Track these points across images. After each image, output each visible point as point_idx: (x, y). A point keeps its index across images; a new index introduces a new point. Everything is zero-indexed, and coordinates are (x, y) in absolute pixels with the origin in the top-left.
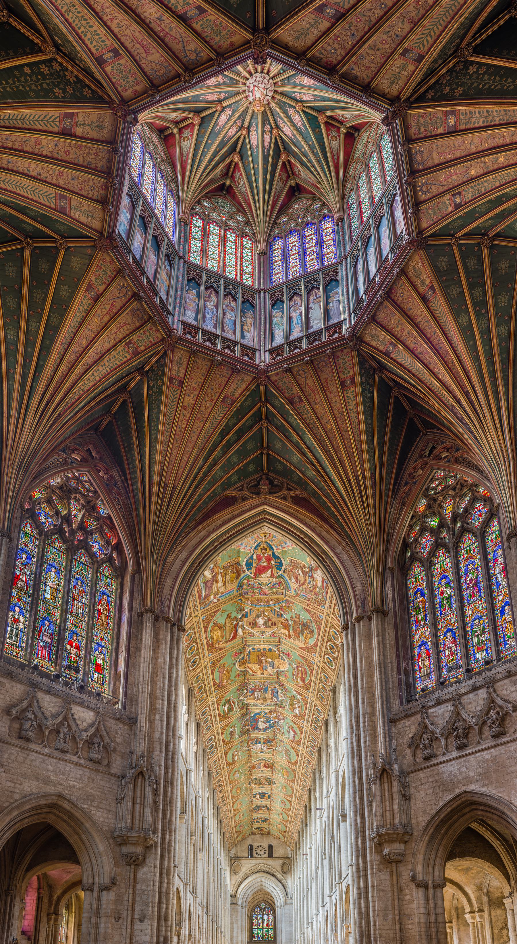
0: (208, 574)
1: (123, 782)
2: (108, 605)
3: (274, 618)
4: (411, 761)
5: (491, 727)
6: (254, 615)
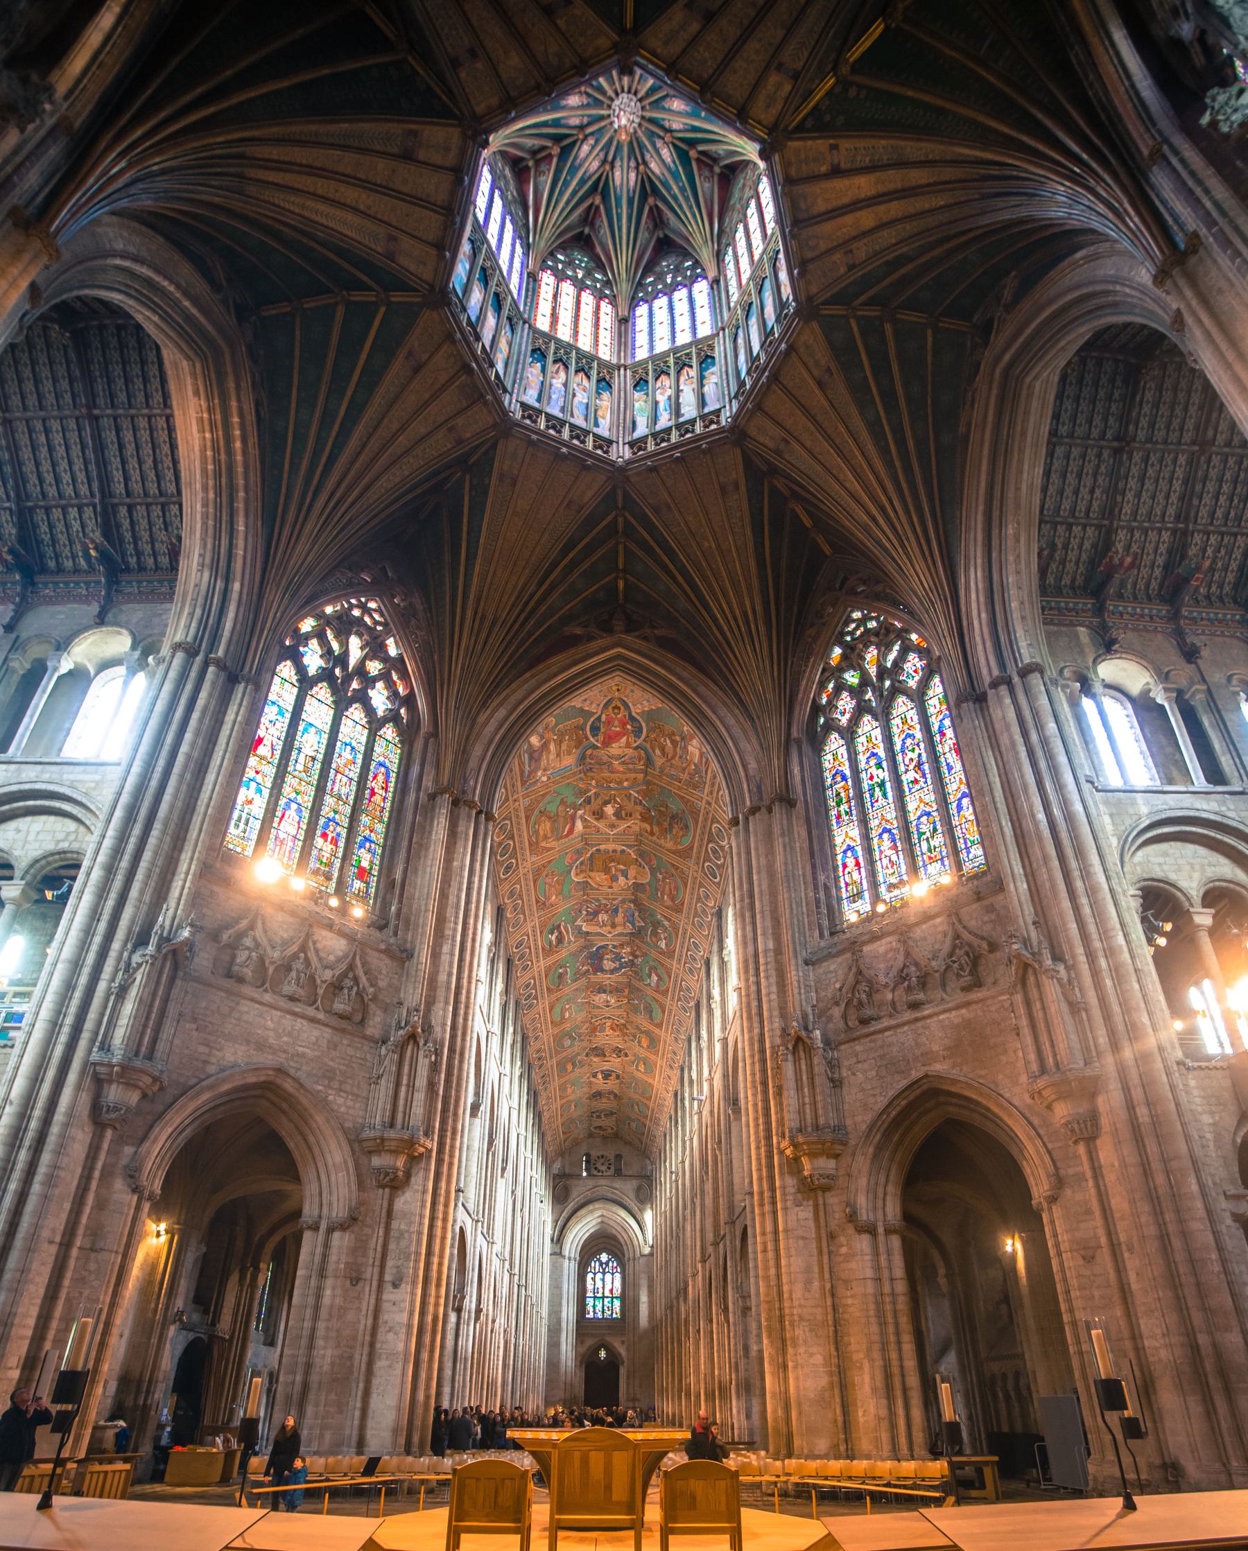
0: (534, 740)
1: (383, 1051)
2: (387, 781)
3: (630, 806)
4: (841, 1024)
5: (958, 975)
6: (600, 801)
